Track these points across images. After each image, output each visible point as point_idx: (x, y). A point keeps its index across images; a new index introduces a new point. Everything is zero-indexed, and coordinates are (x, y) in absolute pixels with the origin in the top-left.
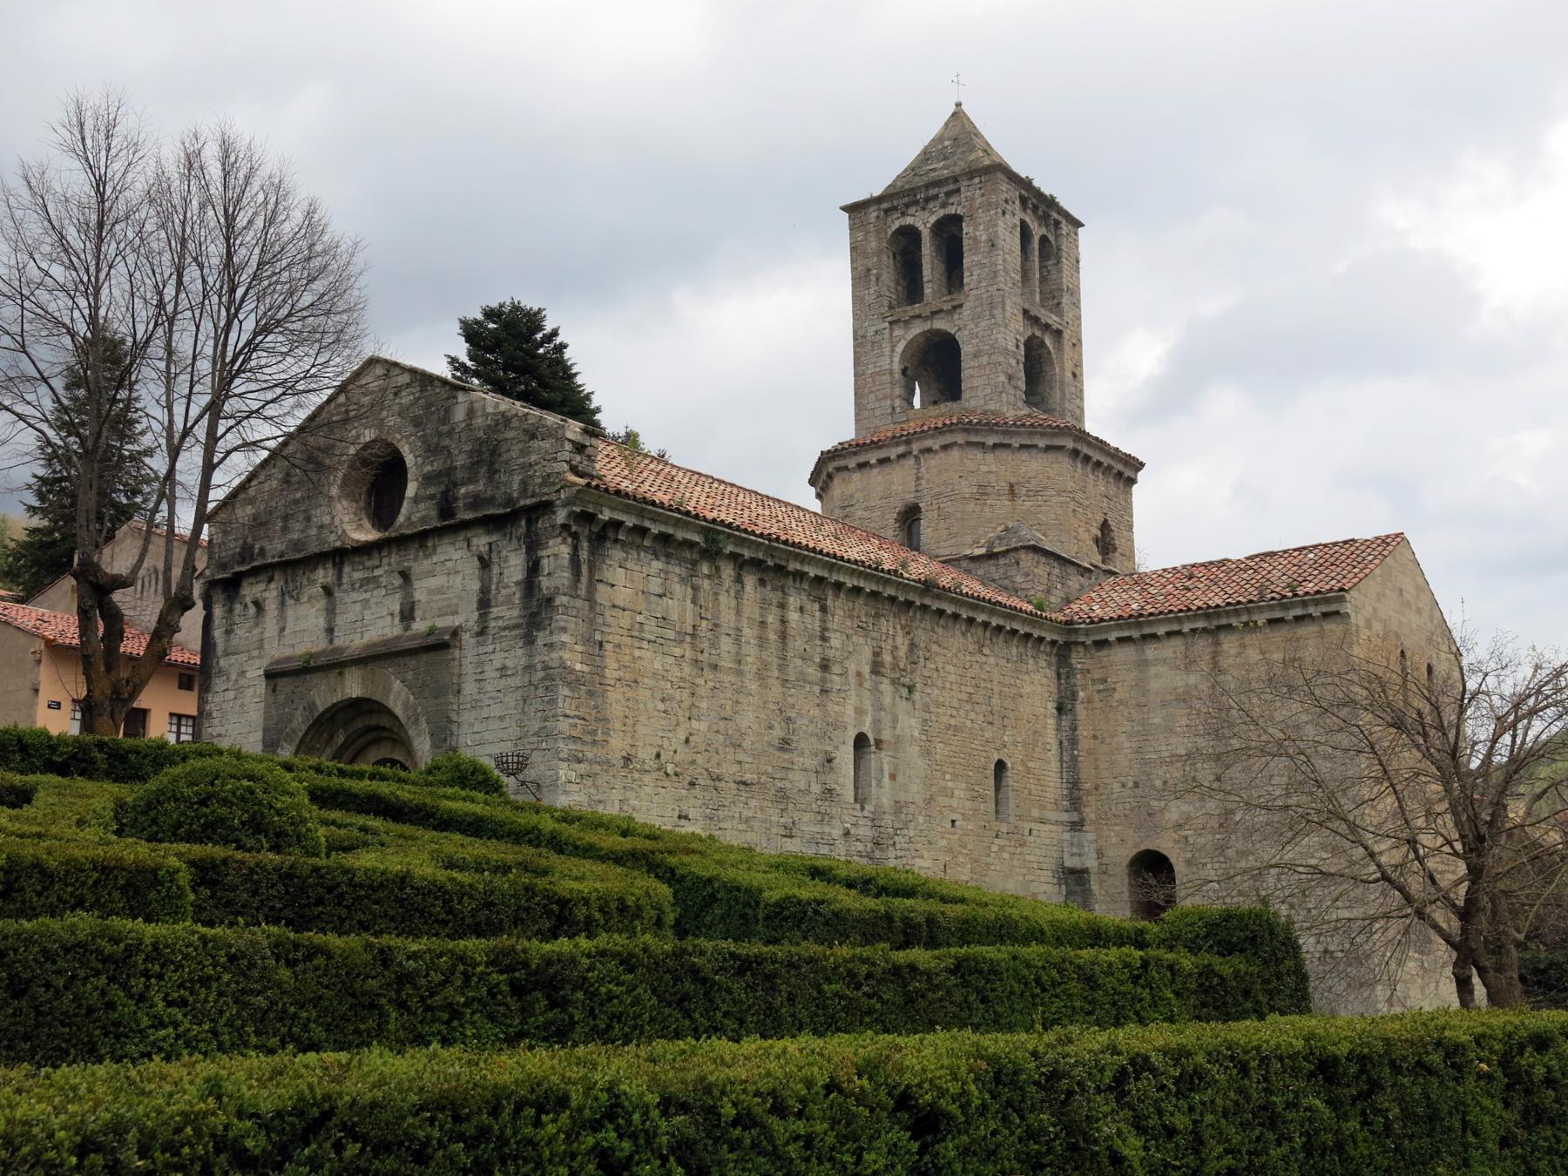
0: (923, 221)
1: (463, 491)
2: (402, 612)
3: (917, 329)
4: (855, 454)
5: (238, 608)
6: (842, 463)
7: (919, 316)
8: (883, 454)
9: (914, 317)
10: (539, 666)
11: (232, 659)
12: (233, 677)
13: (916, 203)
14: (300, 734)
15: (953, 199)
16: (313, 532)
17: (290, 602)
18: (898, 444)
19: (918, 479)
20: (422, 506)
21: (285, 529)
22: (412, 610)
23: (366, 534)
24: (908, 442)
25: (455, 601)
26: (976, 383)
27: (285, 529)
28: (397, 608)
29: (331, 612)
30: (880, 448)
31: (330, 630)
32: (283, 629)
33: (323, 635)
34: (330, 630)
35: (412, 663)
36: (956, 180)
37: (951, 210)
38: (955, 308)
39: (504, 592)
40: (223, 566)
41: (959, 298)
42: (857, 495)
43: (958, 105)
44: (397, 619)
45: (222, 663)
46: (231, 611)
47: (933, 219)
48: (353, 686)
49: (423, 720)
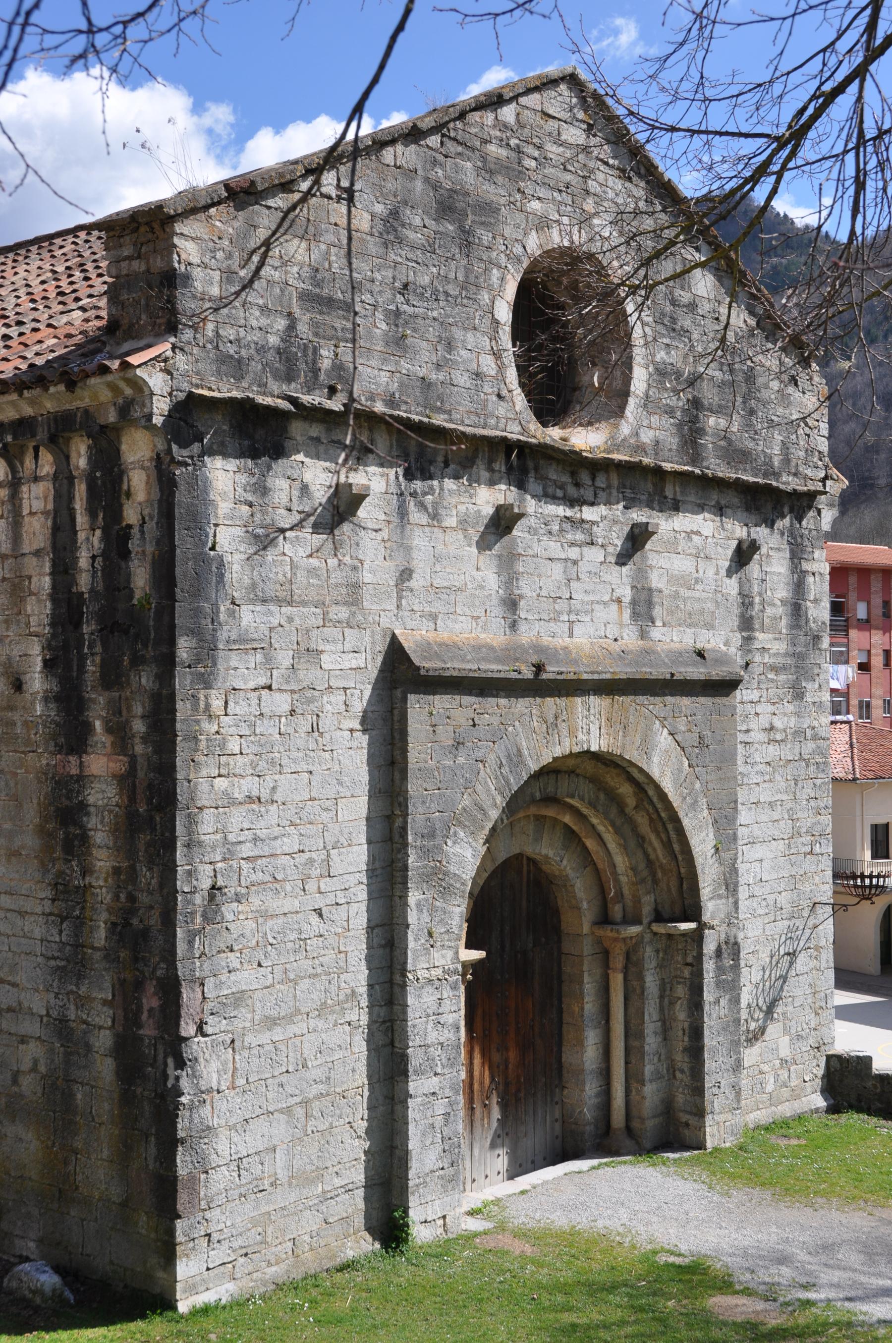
1: (712, 421)
2: (634, 603)
5: (281, 488)
10: (809, 733)
11: (277, 615)
12: (284, 659)
14: (494, 814)
16: (463, 379)
17: (416, 516)
20: (655, 419)
21: (398, 343)
22: (650, 604)
23: (511, 416)
25: (710, 606)
27: (398, 343)
28: (627, 594)
29: (508, 566)
31: (511, 604)
32: (406, 574)
33: (497, 611)
34: (511, 604)
35: (685, 702)
39: (769, 611)
40: (235, 367)
44: (627, 613)
45: (250, 618)
46: (262, 490)
48: (590, 727)
49: (703, 802)
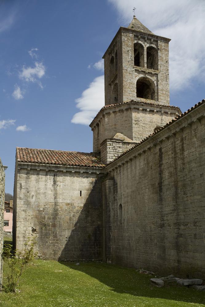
0: (146, 45)
3: (142, 76)
4: (143, 105)
6: (137, 107)
7: (144, 72)
8: (152, 109)
9: (142, 71)
13: (144, 38)
15: (155, 43)
18: (157, 108)
19: (162, 120)
24: (161, 108)
26: (162, 98)
30: (151, 107)
36: (157, 37)
37: (154, 46)
38: (155, 74)
41: (157, 72)
42: (141, 119)
43: (134, 16)
47: (148, 45)
